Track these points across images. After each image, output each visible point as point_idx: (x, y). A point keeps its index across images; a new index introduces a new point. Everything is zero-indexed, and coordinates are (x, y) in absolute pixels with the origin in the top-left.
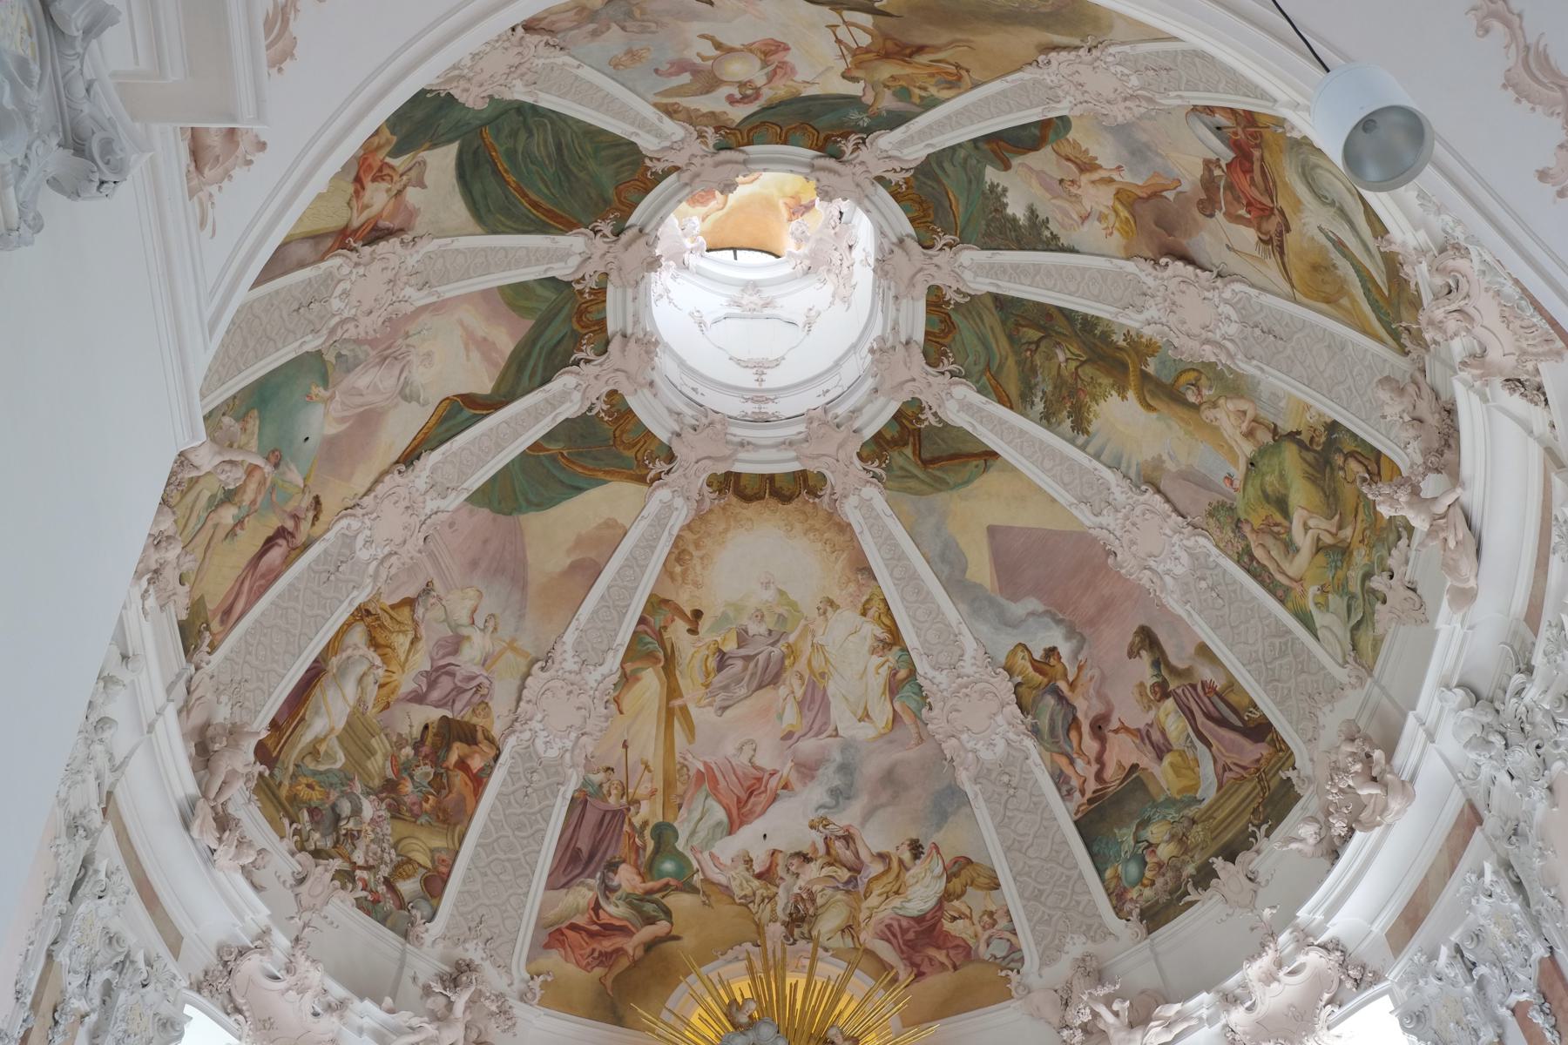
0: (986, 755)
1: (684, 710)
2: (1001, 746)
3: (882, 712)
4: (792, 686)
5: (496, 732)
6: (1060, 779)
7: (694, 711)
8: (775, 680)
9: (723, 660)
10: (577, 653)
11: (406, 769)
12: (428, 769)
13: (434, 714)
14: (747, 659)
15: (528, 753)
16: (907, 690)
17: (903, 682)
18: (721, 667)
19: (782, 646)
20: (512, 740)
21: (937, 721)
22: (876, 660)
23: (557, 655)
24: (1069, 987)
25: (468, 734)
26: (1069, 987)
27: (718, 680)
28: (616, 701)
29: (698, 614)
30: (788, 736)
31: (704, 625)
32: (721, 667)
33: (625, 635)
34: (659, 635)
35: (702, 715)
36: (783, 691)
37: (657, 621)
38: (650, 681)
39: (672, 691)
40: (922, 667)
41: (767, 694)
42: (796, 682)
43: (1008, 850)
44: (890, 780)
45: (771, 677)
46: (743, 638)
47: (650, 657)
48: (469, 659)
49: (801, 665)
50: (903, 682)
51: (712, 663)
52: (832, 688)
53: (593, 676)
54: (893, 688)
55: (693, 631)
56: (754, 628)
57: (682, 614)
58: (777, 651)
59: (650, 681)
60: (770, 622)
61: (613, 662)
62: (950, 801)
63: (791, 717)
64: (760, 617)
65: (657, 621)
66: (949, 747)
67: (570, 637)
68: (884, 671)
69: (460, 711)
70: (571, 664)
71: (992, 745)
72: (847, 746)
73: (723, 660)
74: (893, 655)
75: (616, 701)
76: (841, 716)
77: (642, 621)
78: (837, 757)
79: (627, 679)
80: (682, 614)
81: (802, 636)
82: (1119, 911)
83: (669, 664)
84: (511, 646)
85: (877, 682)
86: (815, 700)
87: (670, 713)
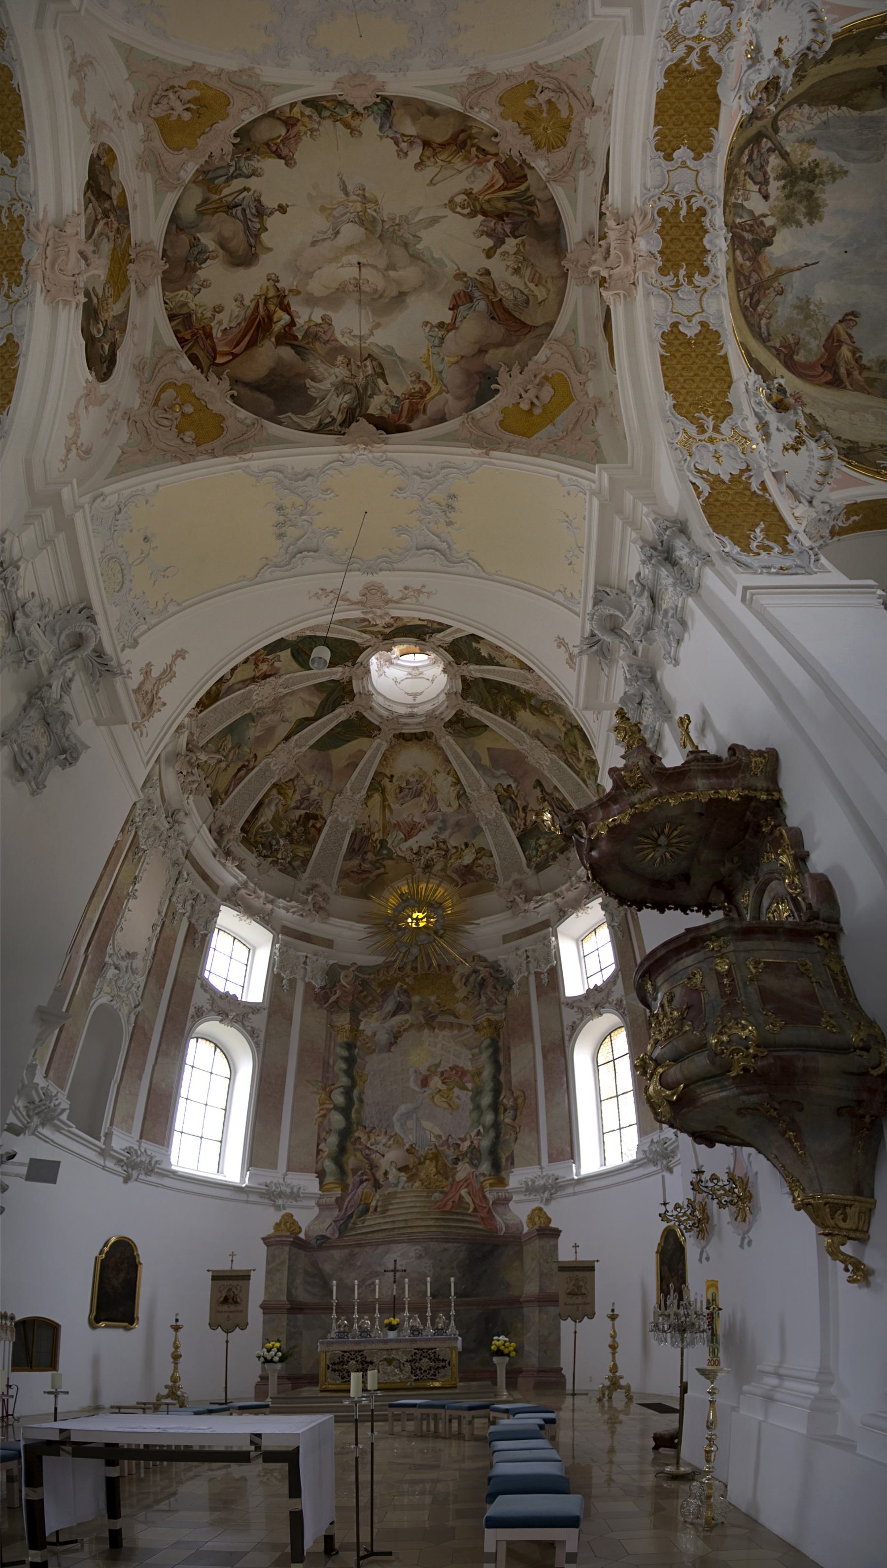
0: (489, 817)
1: (389, 805)
2: (494, 814)
3: (455, 804)
4: (425, 797)
5: (325, 815)
6: (512, 824)
7: (392, 805)
8: (419, 795)
9: (401, 790)
10: (351, 790)
11: (295, 829)
12: (302, 828)
13: (303, 812)
14: (409, 789)
15: (336, 821)
16: (463, 797)
17: (462, 795)
18: (401, 792)
19: (421, 785)
20: (330, 818)
21: (473, 807)
22: (453, 788)
23: (344, 791)
24: (510, 889)
25: (315, 817)
26: (510, 889)
27: (400, 796)
28: (366, 804)
29: (392, 776)
30: (424, 812)
31: (395, 779)
32: (401, 792)
33: (367, 784)
34: (379, 783)
35: (395, 806)
36: (422, 798)
37: (378, 779)
38: (377, 797)
39: (384, 800)
40: (468, 790)
41: (417, 799)
42: (426, 796)
43: (496, 845)
44: (458, 825)
45: (418, 794)
46: (408, 782)
47: (377, 790)
48: (314, 794)
49: (428, 790)
50: (462, 795)
51: (398, 791)
52: (438, 797)
53: (357, 797)
54: (459, 797)
55: (391, 781)
56: (411, 780)
57: (387, 777)
58: (419, 786)
59: (377, 797)
60: (417, 777)
61: (364, 792)
62: (477, 830)
63: (425, 806)
64: (413, 776)
65: (378, 779)
66: (477, 814)
67: (348, 785)
68: (456, 792)
69: (312, 810)
70: (349, 793)
71: (491, 814)
72: (444, 814)
73: (401, 790)
74: (458, 787)
75: (366, 804)
76: (442, 806)
77: (373, 779)
78: (441, 818)
79: (369, 797)
80: (386, 775)
81: (428, 781)
82: (529, 866)
83: (383, 792)
84: (328, 790)
85: (453, 795)
86: (433, 801)
87: (384, 806)
